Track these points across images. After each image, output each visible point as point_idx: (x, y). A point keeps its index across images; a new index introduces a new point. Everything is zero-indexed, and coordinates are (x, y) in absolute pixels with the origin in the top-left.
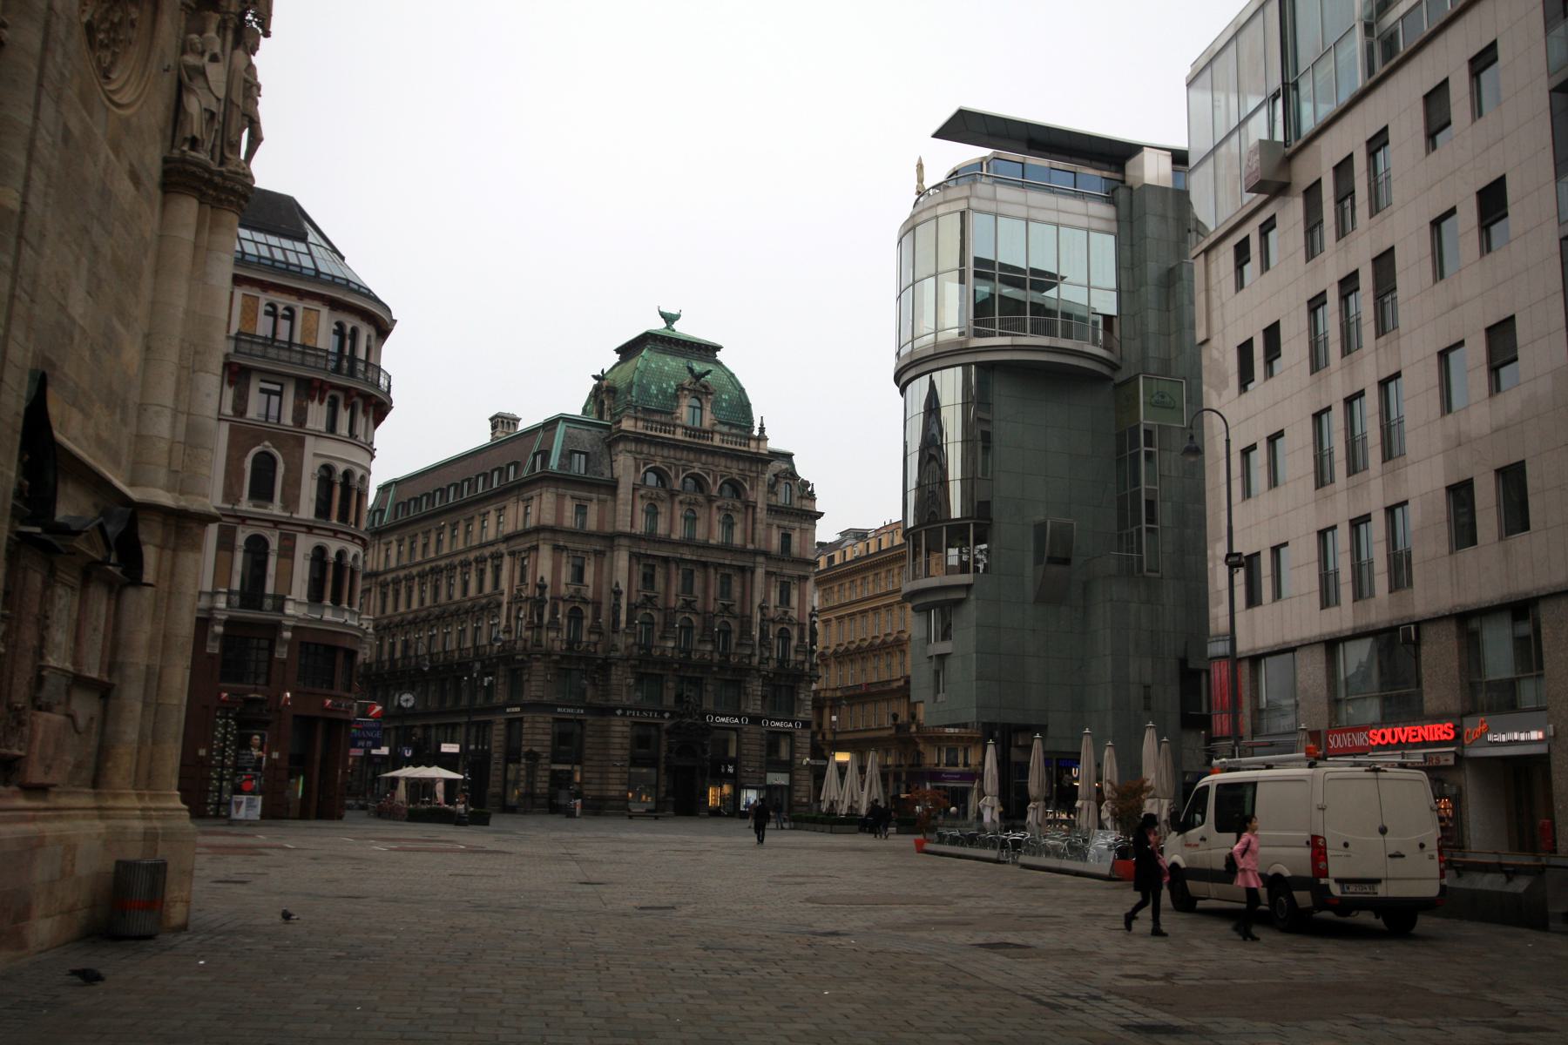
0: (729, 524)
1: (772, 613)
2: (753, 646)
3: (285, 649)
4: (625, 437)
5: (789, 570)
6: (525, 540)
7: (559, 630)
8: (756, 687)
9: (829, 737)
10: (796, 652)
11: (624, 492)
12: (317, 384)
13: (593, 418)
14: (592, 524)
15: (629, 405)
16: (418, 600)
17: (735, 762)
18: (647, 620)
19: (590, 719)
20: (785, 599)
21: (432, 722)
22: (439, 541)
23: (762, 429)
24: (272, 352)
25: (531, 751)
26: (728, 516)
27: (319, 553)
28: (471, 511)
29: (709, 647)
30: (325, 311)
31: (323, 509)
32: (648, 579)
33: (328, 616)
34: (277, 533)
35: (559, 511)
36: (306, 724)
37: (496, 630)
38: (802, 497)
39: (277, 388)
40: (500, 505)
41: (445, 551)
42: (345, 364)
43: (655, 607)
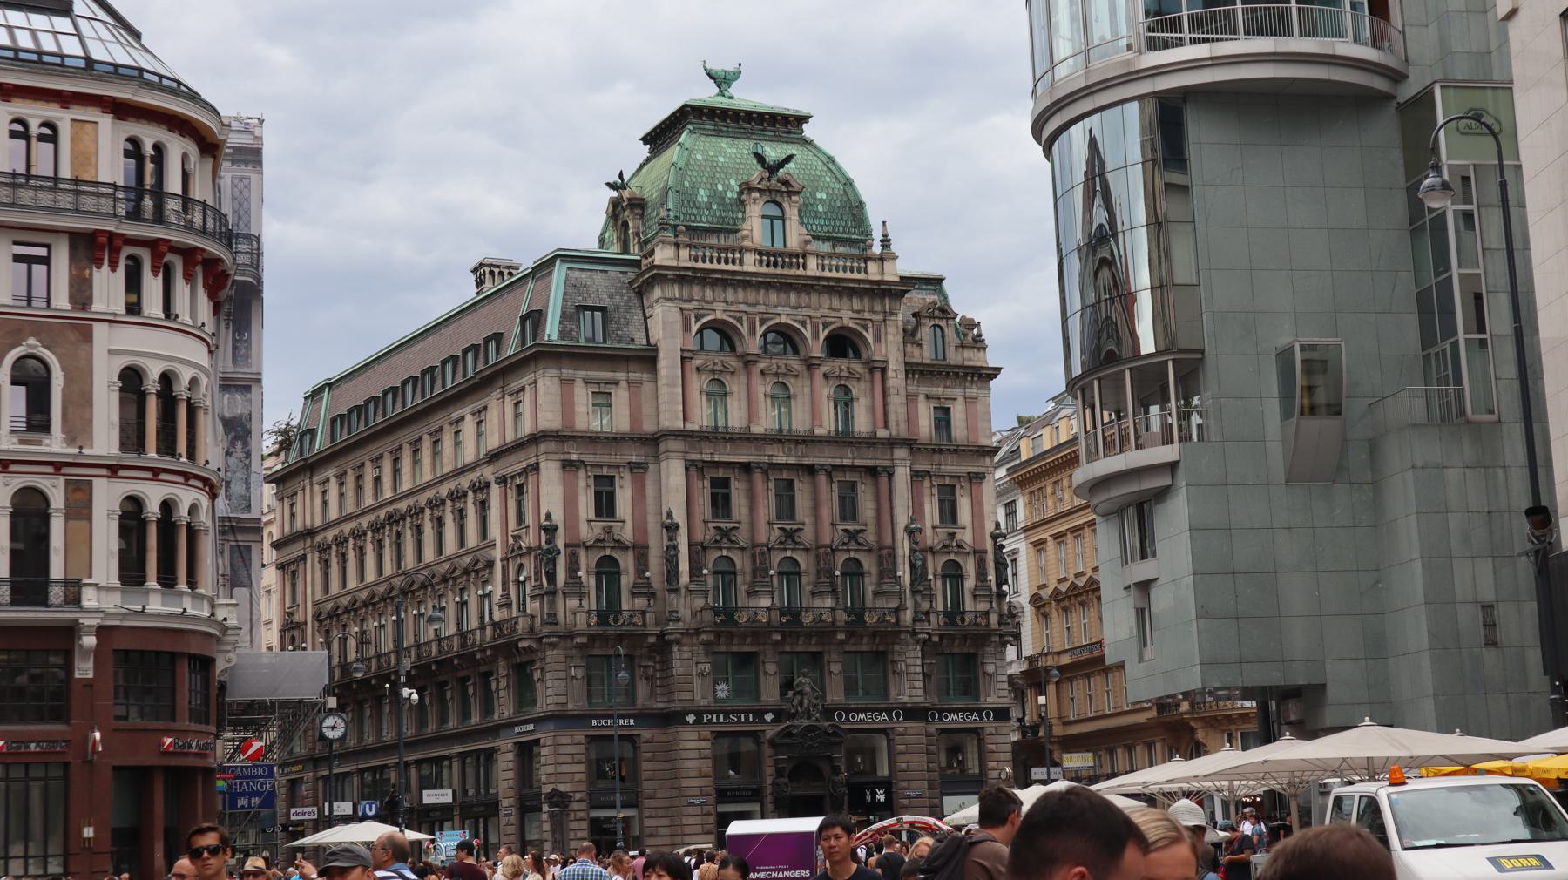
0: (845, 402)
1: (929, 538)
2: (901, 594)
3: (91, 664)
4: (660, 276)
5: (951, 466)
6: (517, 458)
7: (582, 595)
8: (911, 660)
10: (975, 597)
11: (668, 364)
12: (103, 239)
13: (614, 251)
14: (620, 420)
15: (664, 225)
16: (369, 571)
17: (887, 785)
18: (724, 567)
19: (646, 733)
20: (949, 513)
21: (411, 757)
22: (396, 472)
23: (886, 242)
24: (25, 196)
25: (555, 792)
26: (847, 390)
27: (132, 512)
28: (435, 421)
29: (829, 602)
30: (105, 121)
31: (132, 438)
32: (721, 503)
33: (155, 604)
34: (62, 480)
36: (136, 779)
37: (488, 606)
38: (963, 346)
39: (42, 252)
40: (479, 405)
41: (406, 485)
42: (148, 202)
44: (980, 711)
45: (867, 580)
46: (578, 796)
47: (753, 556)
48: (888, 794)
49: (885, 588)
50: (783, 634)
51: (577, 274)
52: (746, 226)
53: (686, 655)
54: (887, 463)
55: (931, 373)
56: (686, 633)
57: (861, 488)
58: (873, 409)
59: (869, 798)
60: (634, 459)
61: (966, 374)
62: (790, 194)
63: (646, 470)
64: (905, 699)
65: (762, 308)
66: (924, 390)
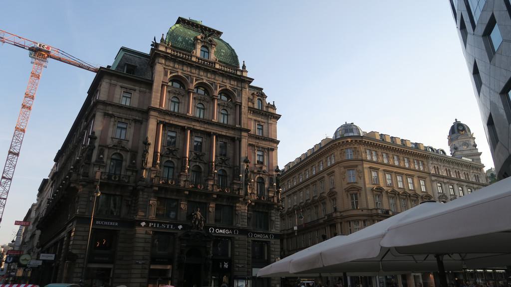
5: (263, 144)
11: (157, 85)
23: (244, 67)
35: (111, 94)
43: (174, 156)
44: (269, 234)
45: (228, 179)
46: (82, 256)
47: (182, 162)
48: (230, 265)
49: (235, 181)
50: (189, 191)
51: (128, 56)
53: (145, 196)
54: (239, 137)
55: (257, 112)
57: (228, 145)
58: (235, 119)
59: (221, 266)
60: (137, 118)
62: (211, 44)
63: (142, 123)
64: (240, 226)
65: (197, 76)
66: (254, 118)
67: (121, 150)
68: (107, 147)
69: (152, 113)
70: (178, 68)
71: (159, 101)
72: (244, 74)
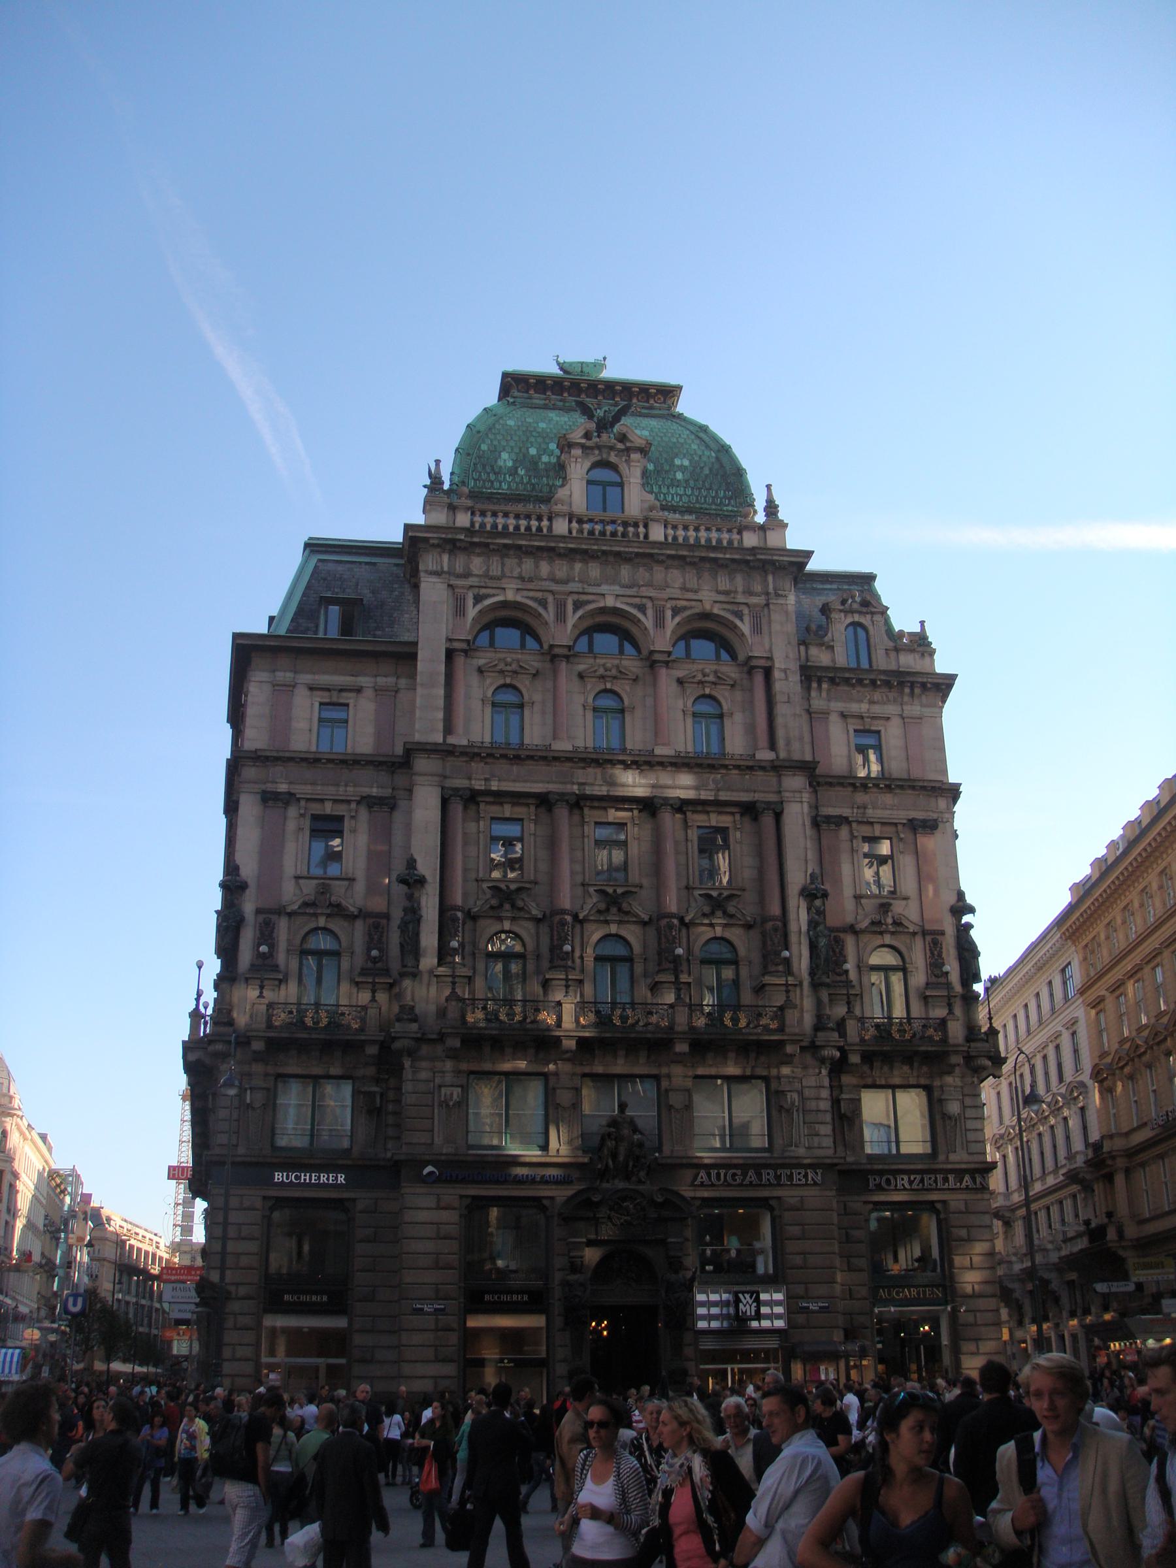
9: (1131, 1231)
10: (925, 999)
11: (430, 660)
23: (771, 508)
46: (242, 1291)
51: (331, 566)
52: (562, 493)
53: (423, 1075)
54: (772, 798)
55: (847, 681)
56: (421, 1040)
58: (751, 729)
60: (374, 791)
61: (901, 684)
64: (801, 1151)
67: (328, 916)
68: (280, 911)
69: (422, 764)
70: (503, 576)
71: (441, 715)
72: (772, 540)
